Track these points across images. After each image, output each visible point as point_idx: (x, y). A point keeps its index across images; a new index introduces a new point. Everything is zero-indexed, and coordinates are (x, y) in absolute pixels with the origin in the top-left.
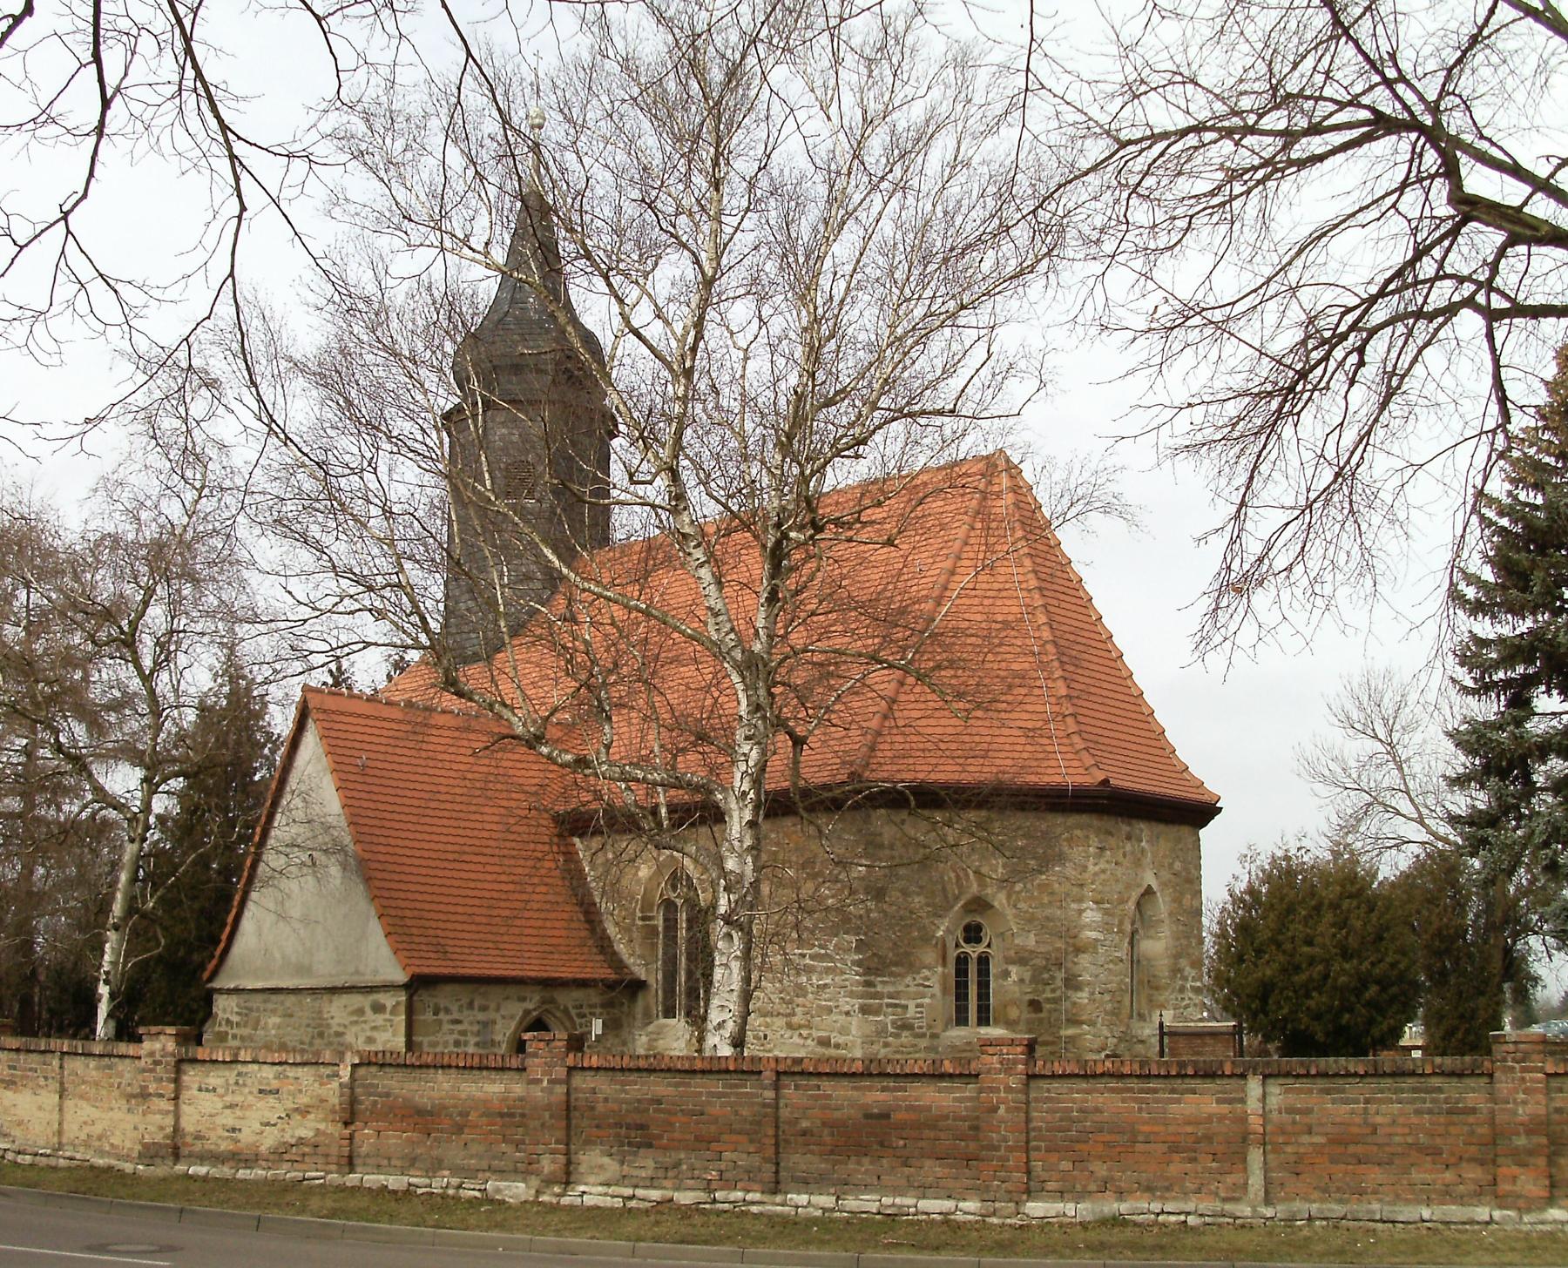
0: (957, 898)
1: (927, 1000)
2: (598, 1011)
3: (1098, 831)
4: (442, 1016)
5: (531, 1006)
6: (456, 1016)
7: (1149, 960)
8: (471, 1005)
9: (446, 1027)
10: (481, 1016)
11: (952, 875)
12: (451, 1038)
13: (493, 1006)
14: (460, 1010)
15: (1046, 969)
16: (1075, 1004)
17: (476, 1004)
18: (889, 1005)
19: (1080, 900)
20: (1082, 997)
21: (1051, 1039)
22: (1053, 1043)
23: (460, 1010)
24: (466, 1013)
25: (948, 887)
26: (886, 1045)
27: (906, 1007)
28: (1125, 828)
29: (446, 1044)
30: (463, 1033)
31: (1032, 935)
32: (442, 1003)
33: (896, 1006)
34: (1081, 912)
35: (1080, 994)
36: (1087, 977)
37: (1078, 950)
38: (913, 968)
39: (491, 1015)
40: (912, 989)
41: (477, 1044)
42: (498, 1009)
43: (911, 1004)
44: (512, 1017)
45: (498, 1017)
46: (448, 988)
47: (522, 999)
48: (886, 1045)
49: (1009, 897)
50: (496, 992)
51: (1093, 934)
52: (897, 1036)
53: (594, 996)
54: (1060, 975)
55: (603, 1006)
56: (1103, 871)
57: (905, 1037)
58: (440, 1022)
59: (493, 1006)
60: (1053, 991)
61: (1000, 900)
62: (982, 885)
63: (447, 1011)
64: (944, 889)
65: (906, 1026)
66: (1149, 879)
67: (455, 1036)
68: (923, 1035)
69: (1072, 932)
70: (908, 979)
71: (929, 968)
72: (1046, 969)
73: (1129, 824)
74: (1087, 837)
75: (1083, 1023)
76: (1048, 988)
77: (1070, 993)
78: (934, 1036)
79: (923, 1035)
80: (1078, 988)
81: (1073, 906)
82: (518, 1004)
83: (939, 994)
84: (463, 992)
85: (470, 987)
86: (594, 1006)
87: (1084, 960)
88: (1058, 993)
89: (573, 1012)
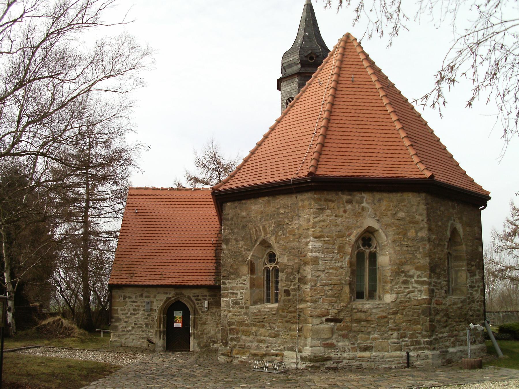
0: (256, 241)
1: (244, 291)
2: (208, 298)
3: (317, 200)
4: (127, 299)
5: (170, 296)
6: (134, 299)
7: (383, 267)
8: (141, 296)
9: (129, 304)
10: (146, 300)
11: (254, 230)
12: (131, 308)
13: (152, 296)
14: (136, 297)
15: (292, 273)
16: (304, 291)
17: (144, 295)
18: (231, 293)
19: (307, 237)
20: (307, 288)
21: (293, 310)
22: (294, 312)
23: (136, 297)
24: (139, 298)
25: (252, 236)
26: (230, 312)
27: (236, 294)
28: (346, 197)
29: (129, 310)
30: (138, 306)
31: (285, 257)
32: (127, 295)
33: (233, 293)
34: (307, 243)
35: (306, 286)
36: (309, 277)
37: (306, 263)
38: (239, 276)
39: (152, 299)
40: (239, 285)
41: (144, 310)
42: (155, 297)
43: (239, 292)
44: (161, 300)
45: (155, 300)
46: (130, 289)
47: (167, 293)
48: (230, 312)
49: (276, 239)
50: (153, 291)
51: (314, 255)
52: (233, 307)
53: (205, 292)
54: (298, 277)
55: (210, 296)
56: (323, 221)
57: (237, 309)
58: (126, 302)
59: (152, 296)
60: (294, 285)
61: (272, 241)
62: (266, 234)
63: (130, 298)
64: (251, 237)
65: (236, 303)
66: (370, 222)
67: (134, 307)
68: (243, 307)
69: (303, 254)
70: (238, 280)
71: (245, 275)
72: (292, 273)
73: (350, 195)
74: (310, 204)
75: (307, 302)
76: (293, 283)
77: (302, 286)
78: (247, 308)
79: (243, 307)
80: (305, 283)
81: (304, 240)
82: (165, 295)
83: (249, 287)
84: (138, 291)
85: (140, 289)
86: (206, 296)
87: (308, 268)
88: (297, 286)
89: (193, 299)
